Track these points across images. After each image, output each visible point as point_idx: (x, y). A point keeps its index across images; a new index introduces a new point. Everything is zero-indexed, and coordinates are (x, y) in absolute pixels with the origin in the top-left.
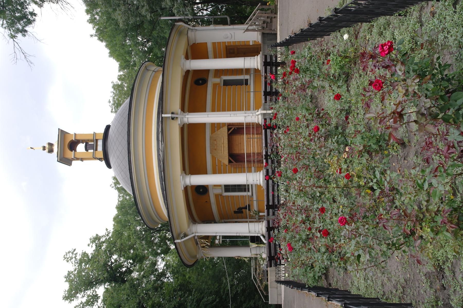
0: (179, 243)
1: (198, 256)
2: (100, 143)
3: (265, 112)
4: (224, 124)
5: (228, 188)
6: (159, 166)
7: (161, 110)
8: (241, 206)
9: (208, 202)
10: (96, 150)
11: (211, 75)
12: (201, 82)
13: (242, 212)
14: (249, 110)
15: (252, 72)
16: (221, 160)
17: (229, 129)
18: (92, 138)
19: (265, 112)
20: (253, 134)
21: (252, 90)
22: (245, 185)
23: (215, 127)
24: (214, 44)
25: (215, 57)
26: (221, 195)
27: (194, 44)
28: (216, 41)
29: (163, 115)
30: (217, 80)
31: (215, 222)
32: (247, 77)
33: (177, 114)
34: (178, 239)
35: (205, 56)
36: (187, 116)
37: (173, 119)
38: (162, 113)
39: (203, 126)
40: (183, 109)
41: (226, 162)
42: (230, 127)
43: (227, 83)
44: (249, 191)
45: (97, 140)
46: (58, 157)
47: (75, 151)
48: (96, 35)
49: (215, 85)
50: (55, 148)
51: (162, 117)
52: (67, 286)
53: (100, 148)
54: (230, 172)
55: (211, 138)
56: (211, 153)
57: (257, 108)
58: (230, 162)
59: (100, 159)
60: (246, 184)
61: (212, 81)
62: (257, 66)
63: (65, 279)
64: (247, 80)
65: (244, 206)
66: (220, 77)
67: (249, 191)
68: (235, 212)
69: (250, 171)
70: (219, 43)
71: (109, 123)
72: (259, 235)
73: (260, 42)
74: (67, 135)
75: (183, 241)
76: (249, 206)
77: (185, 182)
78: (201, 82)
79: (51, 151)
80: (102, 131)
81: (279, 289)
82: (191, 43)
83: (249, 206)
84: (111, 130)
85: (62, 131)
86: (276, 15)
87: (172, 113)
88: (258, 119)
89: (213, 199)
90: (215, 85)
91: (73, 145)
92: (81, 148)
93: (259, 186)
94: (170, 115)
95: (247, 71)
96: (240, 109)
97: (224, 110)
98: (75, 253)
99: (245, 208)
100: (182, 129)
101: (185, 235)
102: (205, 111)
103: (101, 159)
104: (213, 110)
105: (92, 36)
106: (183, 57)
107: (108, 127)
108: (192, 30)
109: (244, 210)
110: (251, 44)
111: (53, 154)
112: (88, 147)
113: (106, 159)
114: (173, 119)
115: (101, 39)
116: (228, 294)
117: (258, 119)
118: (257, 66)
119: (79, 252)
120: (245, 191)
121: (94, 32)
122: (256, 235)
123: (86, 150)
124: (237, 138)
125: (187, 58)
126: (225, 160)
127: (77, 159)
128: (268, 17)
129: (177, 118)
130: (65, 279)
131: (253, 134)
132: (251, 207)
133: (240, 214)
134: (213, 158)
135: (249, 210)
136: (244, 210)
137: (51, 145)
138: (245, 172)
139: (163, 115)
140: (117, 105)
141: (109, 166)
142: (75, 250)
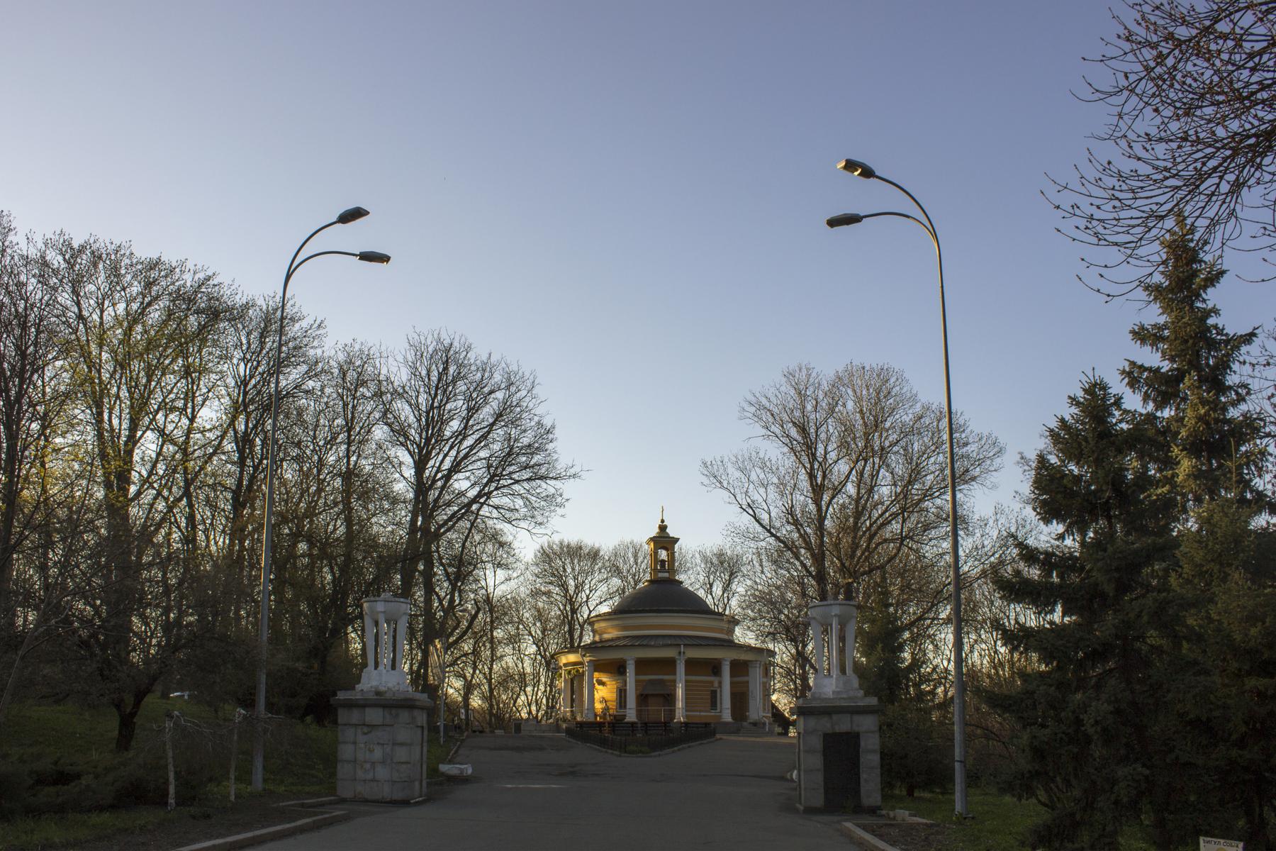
2: (666, 575)
14: (686, 711)
21: (702, 714)
24: (748, 682)
25: (732, 683)
27: (748, 666)
30: (716, 684)
32: (718, 711)
35: (732, 675)
37: (680, 653)
43: (714, 695)
49: (712, 683)
51: (680, 645)
70: (748, 687)
90: (712, 683)
92: (663, 554)
114: (680, 653)
138: (637, 706)
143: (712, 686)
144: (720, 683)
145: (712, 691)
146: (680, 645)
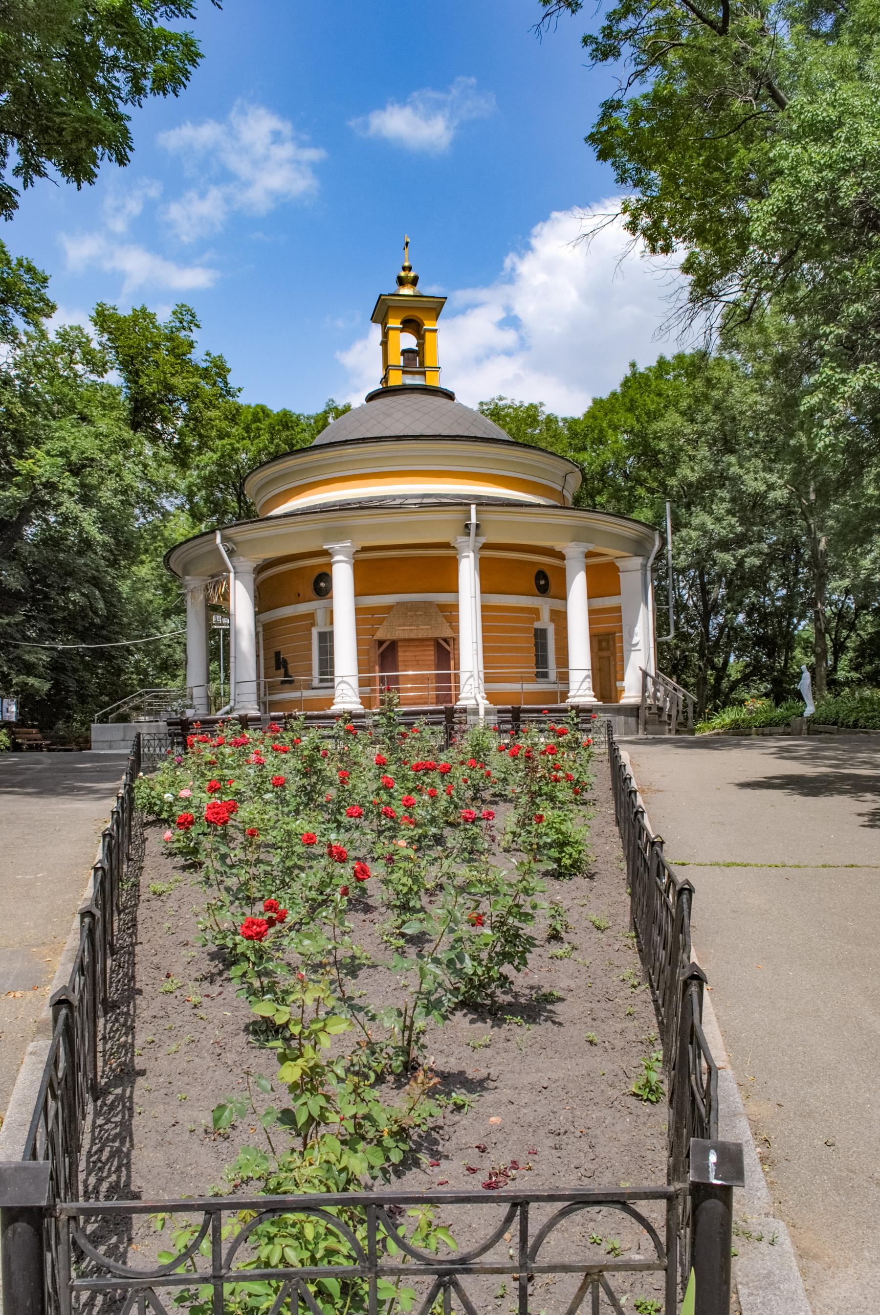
0: (215, 539)
1: (187, 578)
2: (417, 381)
3: (482, 712)
4: (456, 629)
5: (327, 639)
6: (371, 499)
7: (483, 502)
8: (289, 666)
9: (299, 599)
10: (404, 372)
11: (556, 604)
12: (542, 582)
13: (278, 668)
14: (488, 679)
15: (560, 687)
16: (385, 623)
17: (445, 640)
18: (428, 363)
19: (482, 712)
20: (438, 689)
22: (332, 673)
23: (450, 613)
24: (618, 609)
25: (592, 612)
26: (313, 624)
27: (617, 569)
28: (623, 613)
29: (473, 507)
30: (545, 615)
31: (257, 614)
33: (477, 535)
34: (222, 536)
35: (593, 593)
36: (472, 554)
38: (477, 505)
39: (454, 589)
40: (486, 547)
41: (380, 635)
42: (451, 642)
43: (540, 635)
44: (321, 681)
45: (423, 373)
46: (390, 295)
47: (402, 330)
48: (634, 374)
49: (535, 612)
50: (407, 291)
51: (469, 505)
52: (125, 311)
53: (410, 380)
54: (359, 642)
55: (430, 603)
56: (398, 603)
57: (491, 697)
58: (381, 643)
59: (385, 379)
60: (336, 674)
61: (544, 605)
62: (574, 697)
63: (138, 309)
64: (545, 675)
65: (290, 671)
66: (552, 620)
67: (321, 681)
68: (278, 654)
69: (362, 683)
71: (459, 398)
72: (232, 703)
73: (623, 701)
74: (434, 315)
75: (218, 549)
76: (291, 682)
77: (338, 553)
78: (542, 582)
79: (401, 281)
80: (444, 385)
81: (122, 743)
82: (620, 564)
83: (291, 682)
84: (445, 401)
85: (443, 304)
86: (674, 732)
87: (478, 526)
88: (467, 699)
89: (302, 608)
90: (535, 612)
91: (412, 325)
92: (409, 341)
93: (330, 702)
94: (474, 520)
95: (564, 677)
96: (488, 662)
97: (485, 629)
98: (193, 328)
99: (286, 674)
100: (447, 546)
101: (231, 553)
102: (482, 592)
103: (386, 382)
104: (484, 608)
105: (633, 365)
106: (592, 547)
107: (450, 396)
108: (646, 566)
109: (282, 671)
110: (618, 684)
111: (396, 286)
112: (410, 355)
113: (386, 392)
114: (467, 526)
115: (626, 383)
116: (109, 640)
117: (467, 699)
118: (574, 697)
119: (195, 335)
120: (321, 674)
121: (641, 368)
122: (232, 697)
123: (404, 352)
124: (430, 654)
125: (589, 555)
126: (381, 634)
127: (385, 335)
128: (670, 716)
129: (468, 535)
130: (138, 309)
131: (438, 689)
132: (287, 686)
133: (273, 663)
134: (389, 609)
135: (283, 682)
136: (282, 671)
137: (414, 282)
139: (473, 507)
140: (496, 413)
141: (371, 398)
142: (198, 326)
143: (538, 619)
144: (560, 618)
145: (536, 630)
146: (469, 505)
